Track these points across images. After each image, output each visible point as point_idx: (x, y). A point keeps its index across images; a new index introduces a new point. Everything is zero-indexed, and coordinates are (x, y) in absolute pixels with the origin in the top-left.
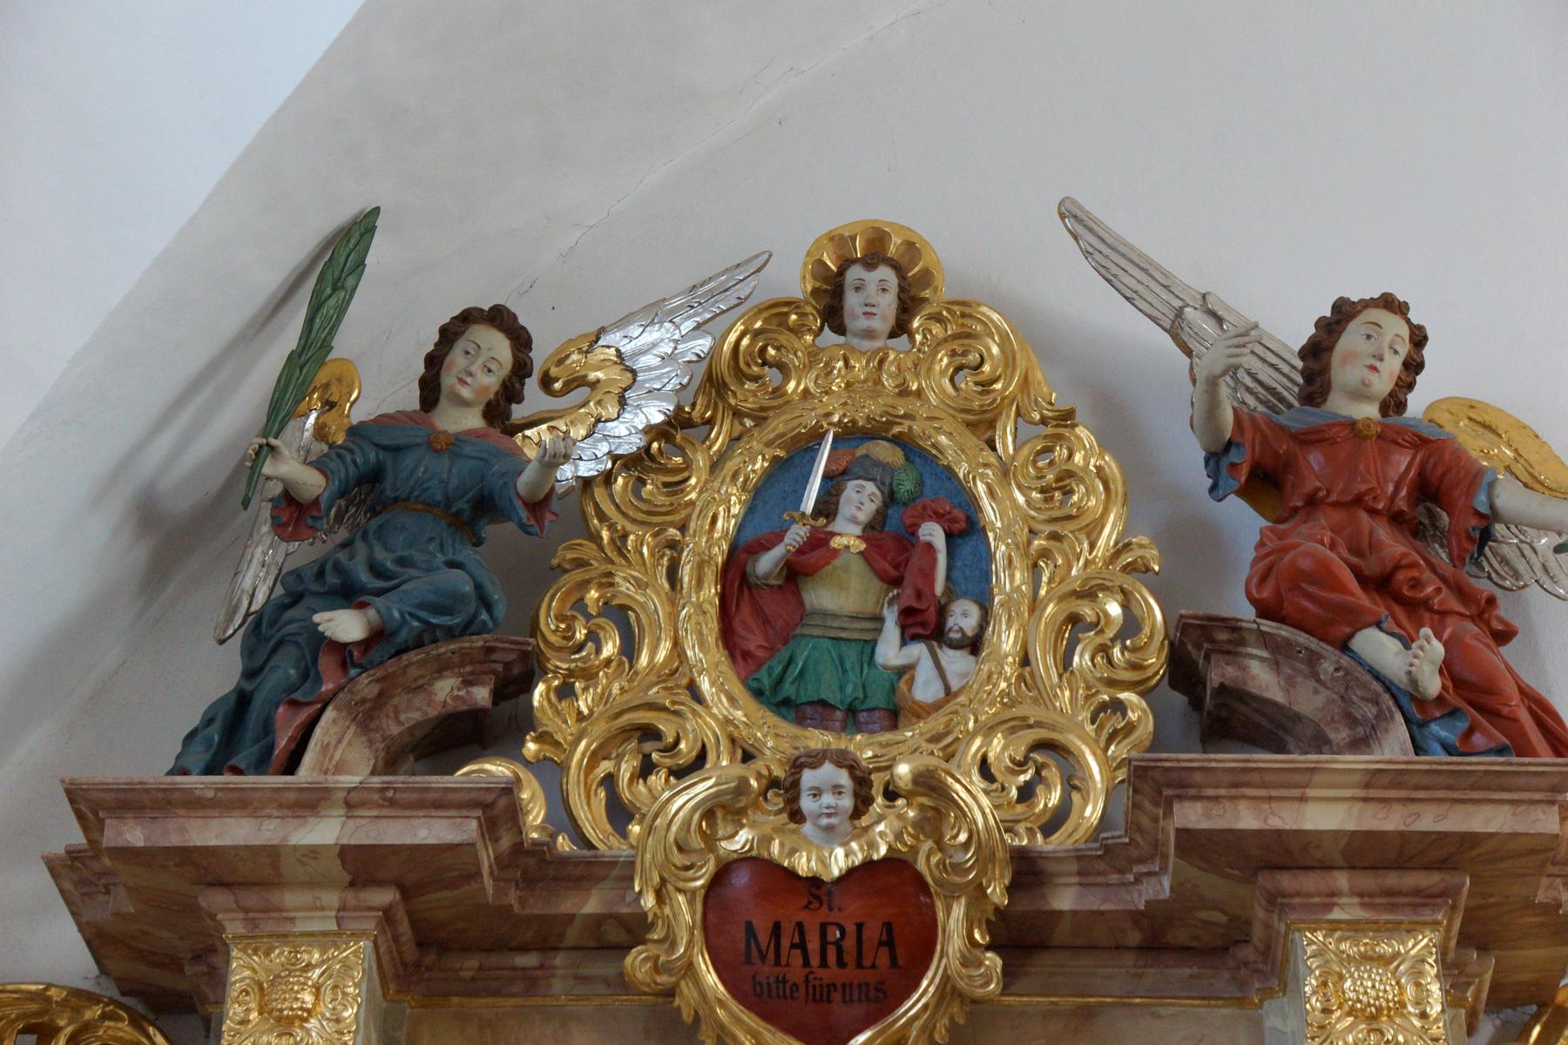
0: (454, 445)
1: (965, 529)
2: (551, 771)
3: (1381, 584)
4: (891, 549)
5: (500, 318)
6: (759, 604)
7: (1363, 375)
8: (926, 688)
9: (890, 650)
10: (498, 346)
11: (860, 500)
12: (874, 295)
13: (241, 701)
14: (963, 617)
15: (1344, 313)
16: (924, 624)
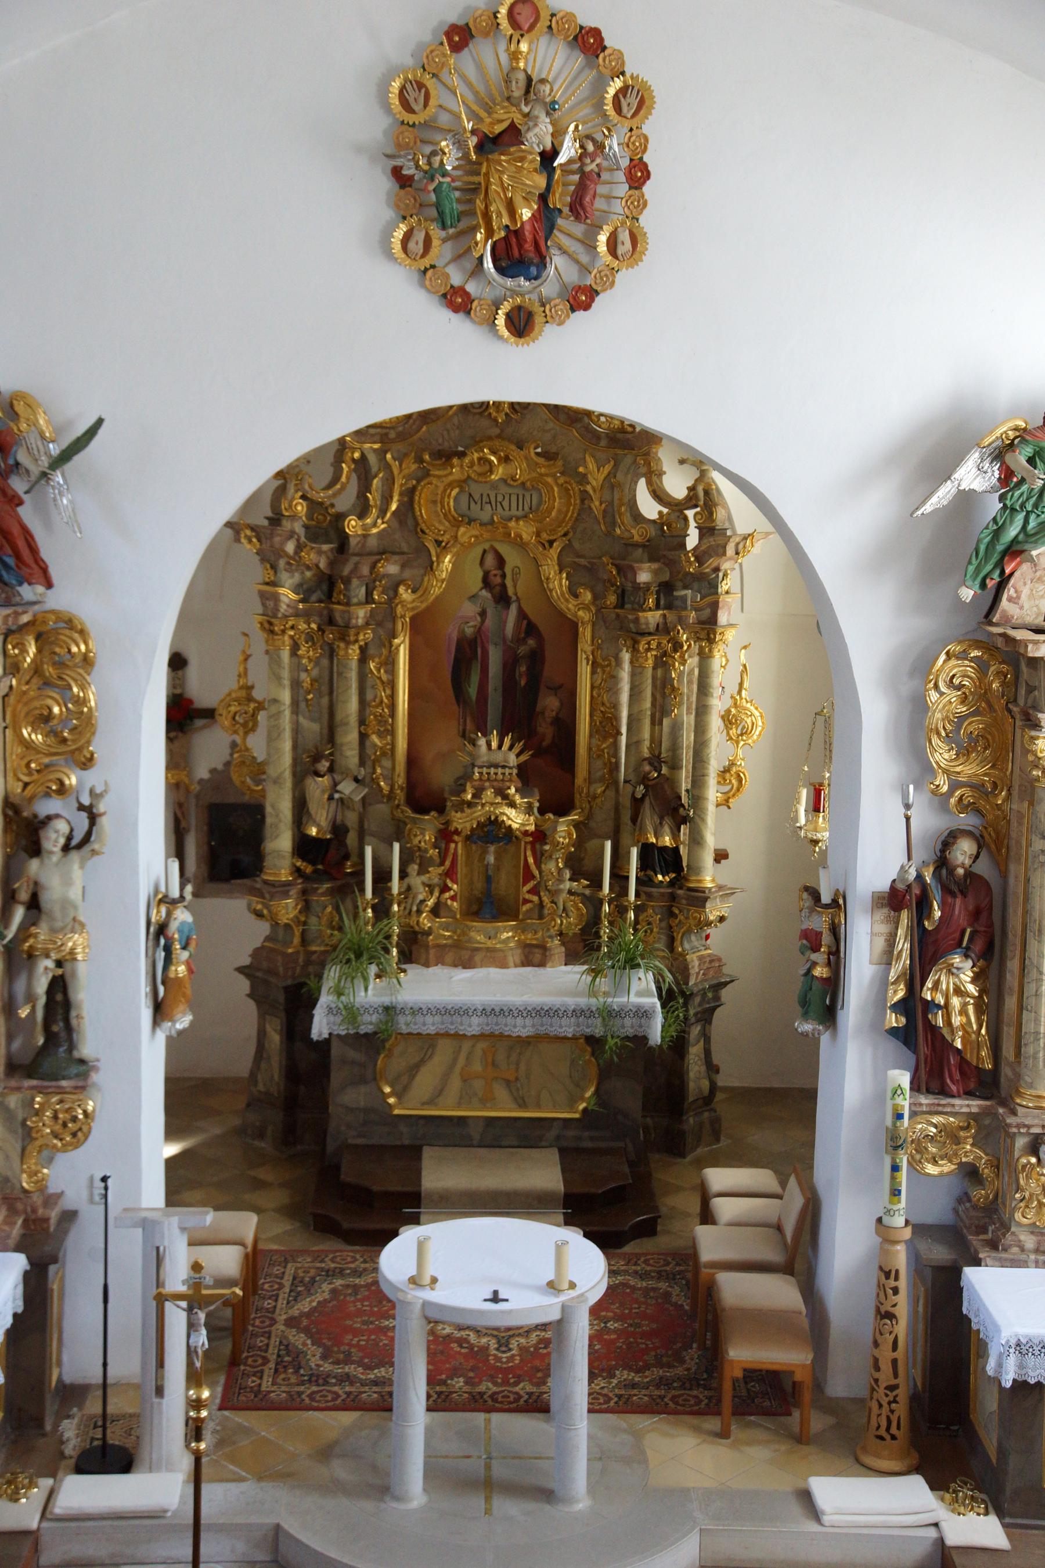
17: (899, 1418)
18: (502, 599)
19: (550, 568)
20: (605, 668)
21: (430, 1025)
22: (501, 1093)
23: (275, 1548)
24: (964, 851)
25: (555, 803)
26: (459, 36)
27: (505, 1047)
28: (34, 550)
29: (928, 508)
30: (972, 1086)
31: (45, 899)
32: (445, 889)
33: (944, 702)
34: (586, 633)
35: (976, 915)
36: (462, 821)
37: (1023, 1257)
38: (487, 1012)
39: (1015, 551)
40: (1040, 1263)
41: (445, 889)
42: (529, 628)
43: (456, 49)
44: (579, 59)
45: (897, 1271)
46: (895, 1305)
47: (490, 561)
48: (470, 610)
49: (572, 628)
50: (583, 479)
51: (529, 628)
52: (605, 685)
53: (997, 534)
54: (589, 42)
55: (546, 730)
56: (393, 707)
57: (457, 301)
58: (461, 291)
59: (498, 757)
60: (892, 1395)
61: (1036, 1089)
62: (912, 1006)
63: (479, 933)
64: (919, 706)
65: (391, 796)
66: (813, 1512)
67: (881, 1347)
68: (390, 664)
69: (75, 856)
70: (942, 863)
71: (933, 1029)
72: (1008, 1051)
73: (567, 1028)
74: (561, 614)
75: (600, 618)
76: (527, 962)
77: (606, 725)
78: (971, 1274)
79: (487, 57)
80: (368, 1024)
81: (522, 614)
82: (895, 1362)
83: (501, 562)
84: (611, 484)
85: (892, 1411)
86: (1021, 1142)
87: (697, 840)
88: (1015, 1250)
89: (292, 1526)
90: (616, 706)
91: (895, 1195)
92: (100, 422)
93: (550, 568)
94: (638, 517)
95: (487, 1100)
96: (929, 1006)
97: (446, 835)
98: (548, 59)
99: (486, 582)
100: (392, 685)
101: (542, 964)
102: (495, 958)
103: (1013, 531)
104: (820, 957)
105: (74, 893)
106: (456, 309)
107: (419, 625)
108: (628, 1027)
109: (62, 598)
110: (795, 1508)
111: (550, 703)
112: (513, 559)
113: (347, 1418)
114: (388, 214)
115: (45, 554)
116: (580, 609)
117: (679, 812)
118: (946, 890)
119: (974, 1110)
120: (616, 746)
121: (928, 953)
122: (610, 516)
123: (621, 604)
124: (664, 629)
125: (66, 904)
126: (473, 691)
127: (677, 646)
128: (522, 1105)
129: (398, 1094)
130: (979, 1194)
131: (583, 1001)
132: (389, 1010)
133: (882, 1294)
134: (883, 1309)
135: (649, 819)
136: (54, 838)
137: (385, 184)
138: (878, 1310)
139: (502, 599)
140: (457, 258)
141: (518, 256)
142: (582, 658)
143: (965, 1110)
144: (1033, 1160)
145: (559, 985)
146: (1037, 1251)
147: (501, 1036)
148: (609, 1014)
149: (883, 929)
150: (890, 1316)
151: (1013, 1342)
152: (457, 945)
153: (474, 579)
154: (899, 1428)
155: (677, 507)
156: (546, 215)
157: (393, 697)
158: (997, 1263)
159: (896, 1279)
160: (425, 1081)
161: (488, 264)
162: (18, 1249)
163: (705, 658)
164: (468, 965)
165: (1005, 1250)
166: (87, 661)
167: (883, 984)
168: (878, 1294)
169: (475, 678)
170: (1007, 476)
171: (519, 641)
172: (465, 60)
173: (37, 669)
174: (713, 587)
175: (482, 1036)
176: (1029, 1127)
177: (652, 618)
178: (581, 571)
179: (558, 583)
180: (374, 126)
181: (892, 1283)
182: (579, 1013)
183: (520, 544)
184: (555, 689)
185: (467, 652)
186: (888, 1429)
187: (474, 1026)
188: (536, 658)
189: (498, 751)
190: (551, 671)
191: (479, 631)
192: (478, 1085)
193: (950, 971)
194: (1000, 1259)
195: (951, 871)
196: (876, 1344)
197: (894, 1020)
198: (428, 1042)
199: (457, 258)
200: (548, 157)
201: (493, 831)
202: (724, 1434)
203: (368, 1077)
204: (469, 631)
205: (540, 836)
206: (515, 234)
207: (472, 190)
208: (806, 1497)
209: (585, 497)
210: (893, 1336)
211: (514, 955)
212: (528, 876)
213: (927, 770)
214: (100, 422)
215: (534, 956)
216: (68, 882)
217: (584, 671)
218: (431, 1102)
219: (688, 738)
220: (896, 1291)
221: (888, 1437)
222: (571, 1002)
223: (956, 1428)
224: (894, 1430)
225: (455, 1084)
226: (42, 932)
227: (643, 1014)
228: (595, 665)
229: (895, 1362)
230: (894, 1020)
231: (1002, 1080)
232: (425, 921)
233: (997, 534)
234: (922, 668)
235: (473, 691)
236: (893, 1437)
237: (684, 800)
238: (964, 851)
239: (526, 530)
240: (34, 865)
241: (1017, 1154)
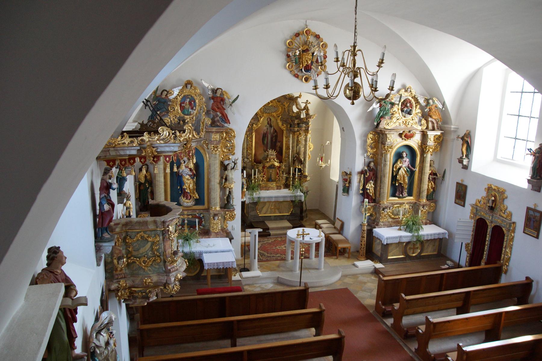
0: (163, 98)
1: (195, 102)
2: (170, 118)
3: (218, 108)
4: (190, 103)
5: (166, 90)
6: (182, 108)
7: (219, 92)
8: (192, 113)
9: (190, 110)
10: (166, 92)
11: (188, 100)
12: (189, 86)
13: (152, 115)
14: (194, 108)
15: (218, 89)
16: (192, 109)
18: (271, 126)
19: (279, 121)
20: (288, 137)
21: (266, 200)
22: (277, 211)
23: (278, 280)
24: (372, 164)
25: (280, 162)
26: (297, 35)
27: (278, 204)
28: (227, 117)
29: (369, 110)
31: (228, 178)
32: (264, 177)
33: (369, 141)
34: (285, 132)
35: (373, 174)
36: (267, 165)
38: (276, 197)
39: (382, 117)
41: (264, 177)
42: (275, 131)
43: (298, 36)
44: (315, 39)
47: (269, 120)
48: (265, 128)
49: (283, 131)
50: (284, 106)
51: (275, 131)
52: (288, 142)
53: (379, 114)
54: (317, 37)
55: (278, 149)
56: (252, 146)
57: (296, 76)
58: (297, 74)
59: (272, 154)
62: (364, 189)
63: (269, 184)
64: (365, 141)
65: (251, 161)
66: (356, 266)
68: (252, 138)
69: (233, 170)
70: (368, 166)
71: (367, 193)
72: (378, 195)
73: (289, 199)
74: (281, 129)
75: (287, 129)
76: (277, 189)
77: (288, 148)
78: (374, 229)
79: (302, 38)
80: (256, 200)
81: (274, 129)
83: (270, 120)
84: (289, 106)
86: (381, 209)
87: (305, 167)
89: (280, 276)
90: (289, 144)
92: (238, 96)
93: (279, 121)
94: (293, 112)
95: (275, 212)
96: (367, 189)
97: (264, 167)
98: (311, 39)
99: (268, 124)
100: (252, 142)
101: (280, 189)
102: (273, 189)
103: (381, 114)
104: (347, 183)
105: (233, 177)
106: (296, 77)
107: (256, 131)
108: (298, 198)
109: (231, 126)
110: (353, 267)
111: (279, 144)
112: (273, 119)
113: (278, 262)
114: (285, 62)
115: (229, 118)
116: (284, 128)
117: (301, 163)
118: (369, 171)
120: (289, 151)
121: (366, 181)
122: (289, 111)
123: (291, 127)
124: (298, 131)
125: (232, 178)
126: (266, 142)
127: (300, 134)
128: (280, 213)
129: (260, 212)
130: (372, 218)
131: (291, 195)
132: (259, 198)
135: (296, 163)
136: (229, 167)
137: (285, 57)
139: (271, 126)
140: (296, 69)
141: (308, 69)
142: (284, 136)
145: (284, 193)
147: (270, 202)
148: (295, 197)
149: (359, 177)
152: (266, 187)
153: (266, 123)
155: (300, 110)
156: (312, 62)
157: (252, 144)
160: (264, 210)
161: (303, 70)
162: (227, 237)
163: (306, 135)
164: (268, 190)
166: (234, 137)
167: (359, 186)
169: (266, 140)
170: (381, 106)
171: (274, 133)
172: (298, 38)
173: (226, 138)
174: (308, 124)
175: (274, 202)
177: (296, 129)
178: (284, 121)
179: (280, 124)
180: (284, 48)
182: (290, 197)
183: (274, 116)
184: (279, 142)
185: (265, 136)
187: (273, 200)
188: (276, 136)
189: (272, 153)
190: (279, 139)
191: (267, 132)
192: (273, 210)
193: (370, 183)
195: (370, 167)
197: (361, 192)
198: (265, 203)
199: (296, 69)
200: (313, 54)
201: (273, 166)
202: (337, 258)
203: (255, 209)
204: (265, 132)
205: (279, 167)
206: (307, 65)
207: (300, 58)
208: (354, 265)
209: (285, 108)
211: (275, 188)
212: (277, 174)
213: (366, 151)
214: (238, 96)
215: (279, 188)
216: (232, 175)
217: (284, 138)
218: (265, 214)
219: (302, 149)
222: (289, 195)
225: (269, 210)
226: (227, 183)
227: (300, 196)
228: (286, 138)
230: (361, 192)
232: (261, 182)
233: (379, 114)
234: (366, 136)
235: (266, 142)
237: (303, 159)
238: (372, 164)
239: (274, 114)
240: (226, 172)
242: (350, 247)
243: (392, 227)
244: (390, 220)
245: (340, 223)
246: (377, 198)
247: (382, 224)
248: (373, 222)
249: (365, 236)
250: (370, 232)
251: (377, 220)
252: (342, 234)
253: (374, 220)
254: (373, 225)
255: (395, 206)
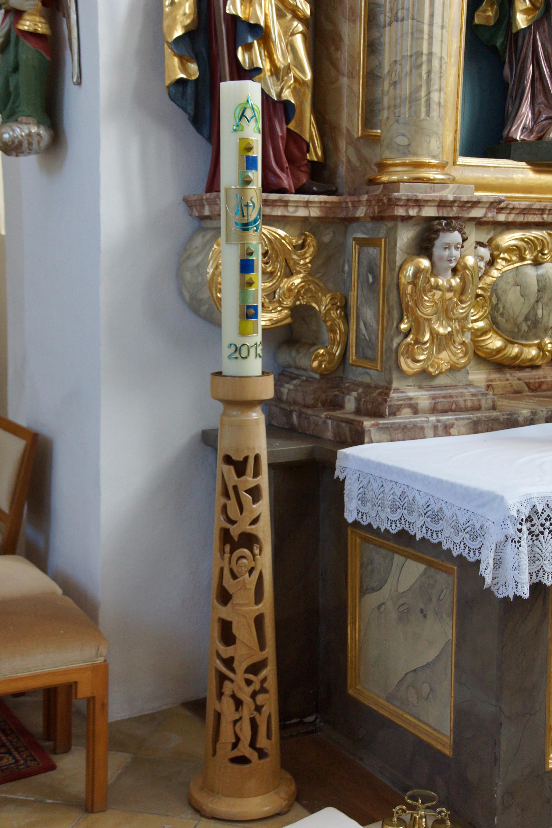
17: (269, 717)
30: (304, 179)
37: (419, 419)
40: (440, 429)
45: (257, 458)
46: (255, 521)
60: (256, 680)
61: (415, 154)
67: (236, 600)
78: (351, 458)
82: (259, 620)
85: (258, 709)
86: (405, 236)
88: (406, 411)
91: (248, 317)
119: (315, 212)
130: (317, 360)
133: (232, 505)
134: (235, 531)
138: (226, 536)
143: (302, 213)
144: (425, 263)
146: (434, 410)
150: (249, 540)
151: (526, 512)
154: (269, 737)
158: (384, 436)
159: (256, 474)
165: (393, 414)
168: (224, 508)
176: (418, 203)
181: (249, 481)
186: (253, 744)
194: (386, 429)
196: (224, 597)
210: (255, 575)
220: (255, 493)
221: (253, 755)
223: (311, 719)
224: (262, 742)
229: (259, 620)
231: (342, 170)
236: (262, 754)
241: (399, 259)
242: (101, 671)
243: (512, 422)
244: (479, 376)
245: (15, 447)
246: (345, 153)
247: (422, 397)
248: (326, 389)
249: (264, 531)
250: (308, 489)
251: (357, 375)
252: (39, 558)
253: (335, 379)
254: (326, 422)
255: (509, 239)
